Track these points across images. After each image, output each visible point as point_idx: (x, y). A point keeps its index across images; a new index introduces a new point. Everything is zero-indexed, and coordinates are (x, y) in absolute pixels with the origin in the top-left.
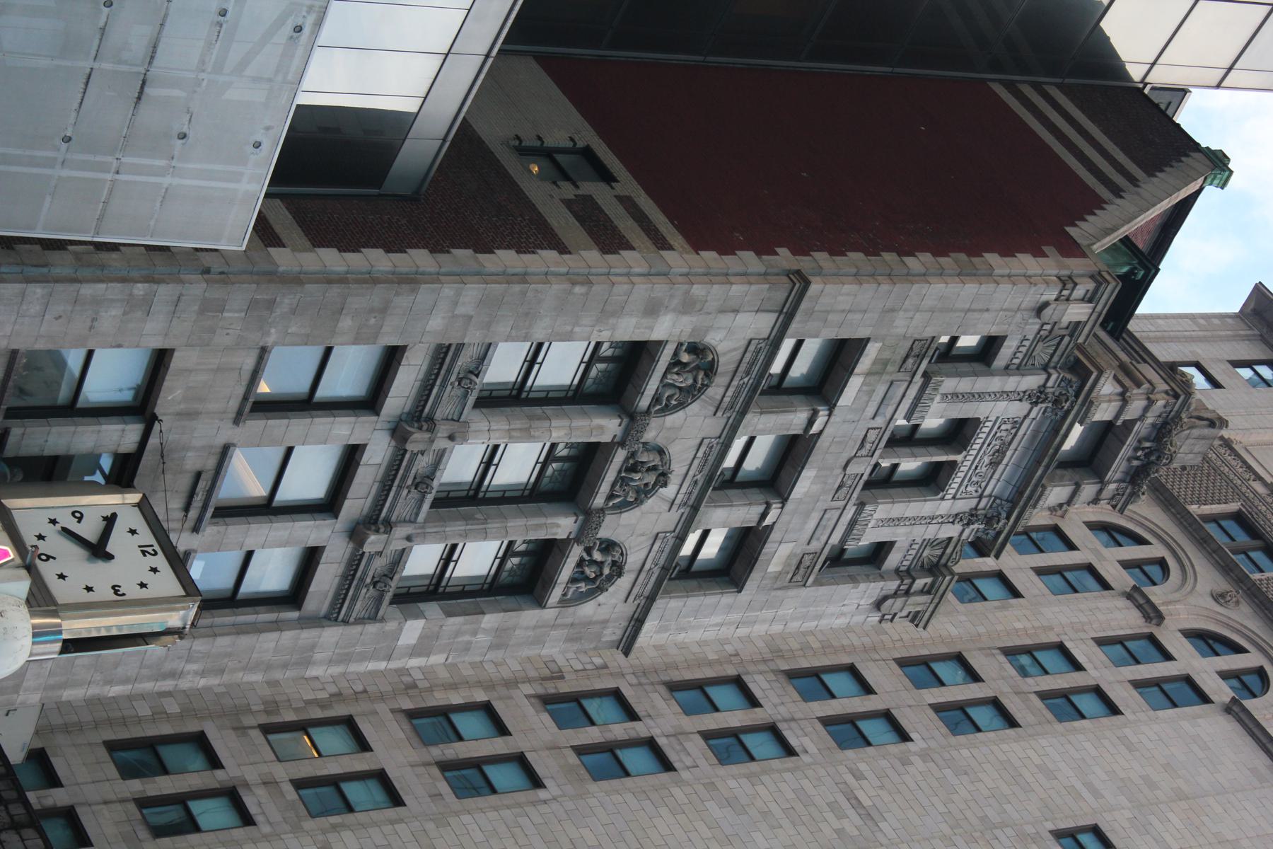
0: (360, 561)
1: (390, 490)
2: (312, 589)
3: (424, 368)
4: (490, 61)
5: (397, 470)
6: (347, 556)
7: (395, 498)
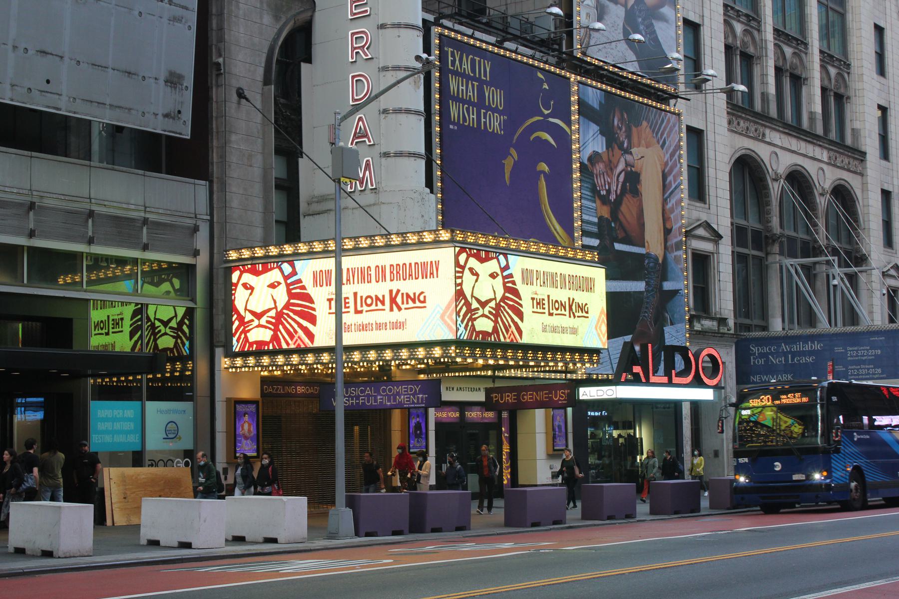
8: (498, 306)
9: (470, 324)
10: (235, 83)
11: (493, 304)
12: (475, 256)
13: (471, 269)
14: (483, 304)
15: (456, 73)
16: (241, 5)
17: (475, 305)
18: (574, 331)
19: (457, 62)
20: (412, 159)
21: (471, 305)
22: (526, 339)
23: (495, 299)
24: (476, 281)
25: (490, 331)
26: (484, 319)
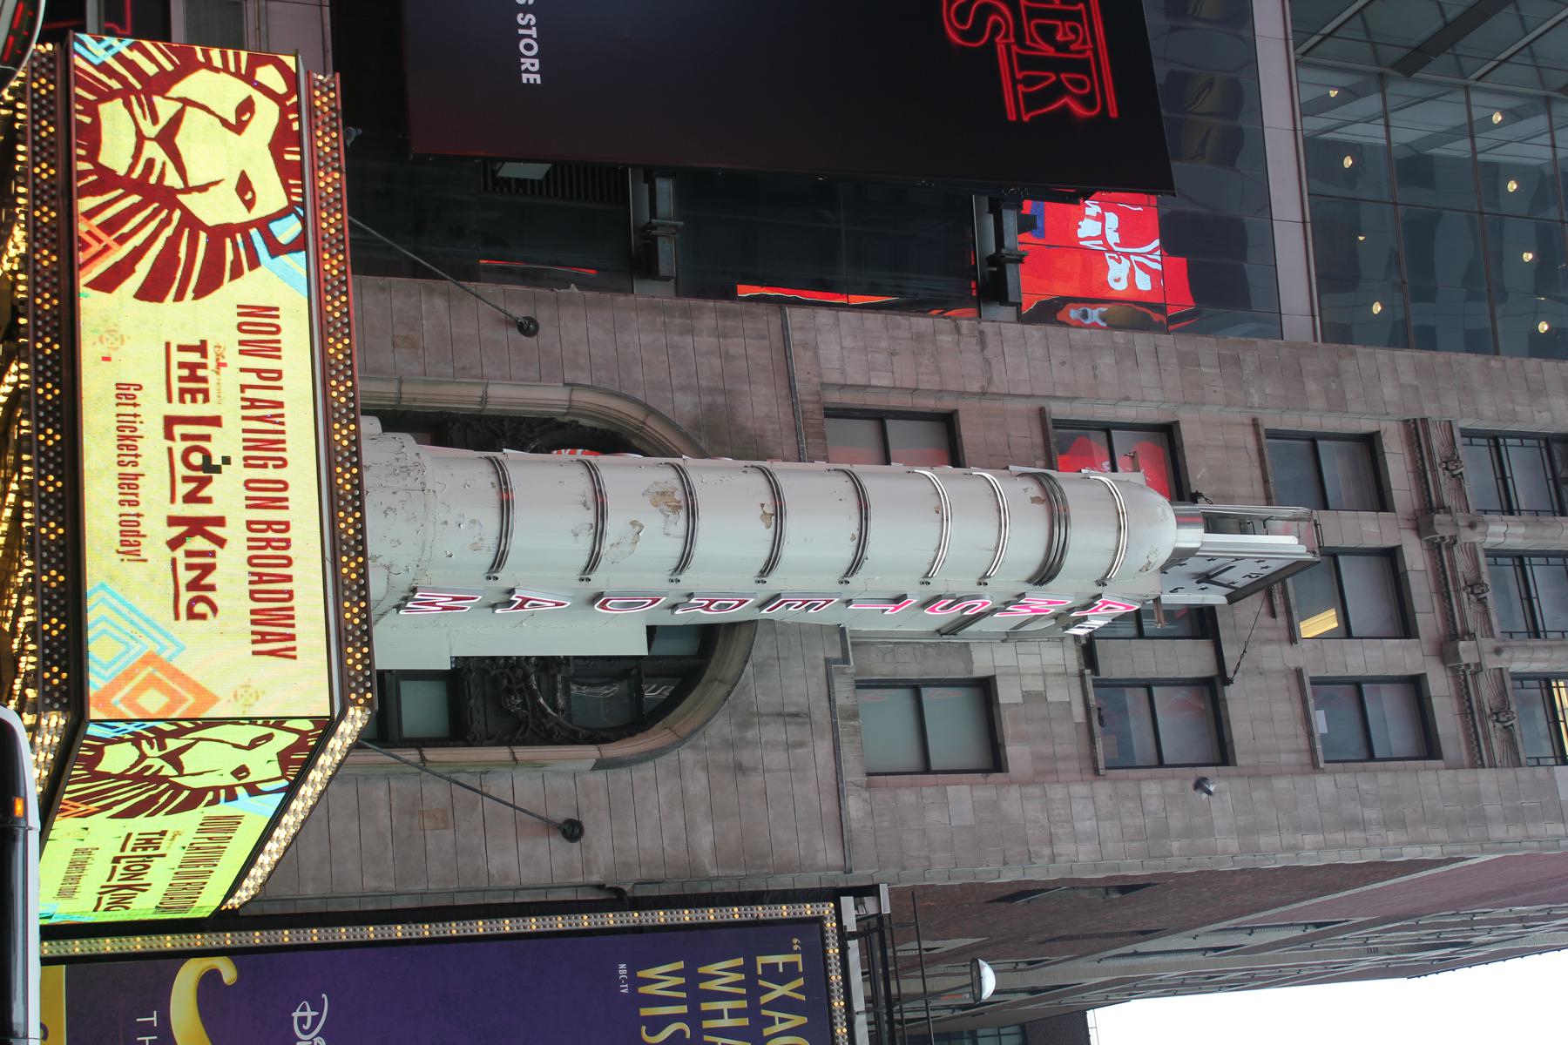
0: (1467, 687)
1: (1449, 597)
2: (1440, 731)
3: (1407, 457)
4: (1309, 226)
5: (1444, 572)
6: (1452, 687)
7: (1460, 605)
8: (167, 198)
9: (115, 85)
10: (543, 315)
11: (173, 179)
12: (284, 123)
13: (247, 107)
14: (167, 138)
15: (753, 990)
16: (689, 339)
17: (166, 109)
18: (130, 538)
19: (780, 991)
20: (493, 478)
21: (163, 93)
22: (92, 304)
23: (188, 190)
24: (225, 123)
25: (105, 159)
26: (132, 140)
